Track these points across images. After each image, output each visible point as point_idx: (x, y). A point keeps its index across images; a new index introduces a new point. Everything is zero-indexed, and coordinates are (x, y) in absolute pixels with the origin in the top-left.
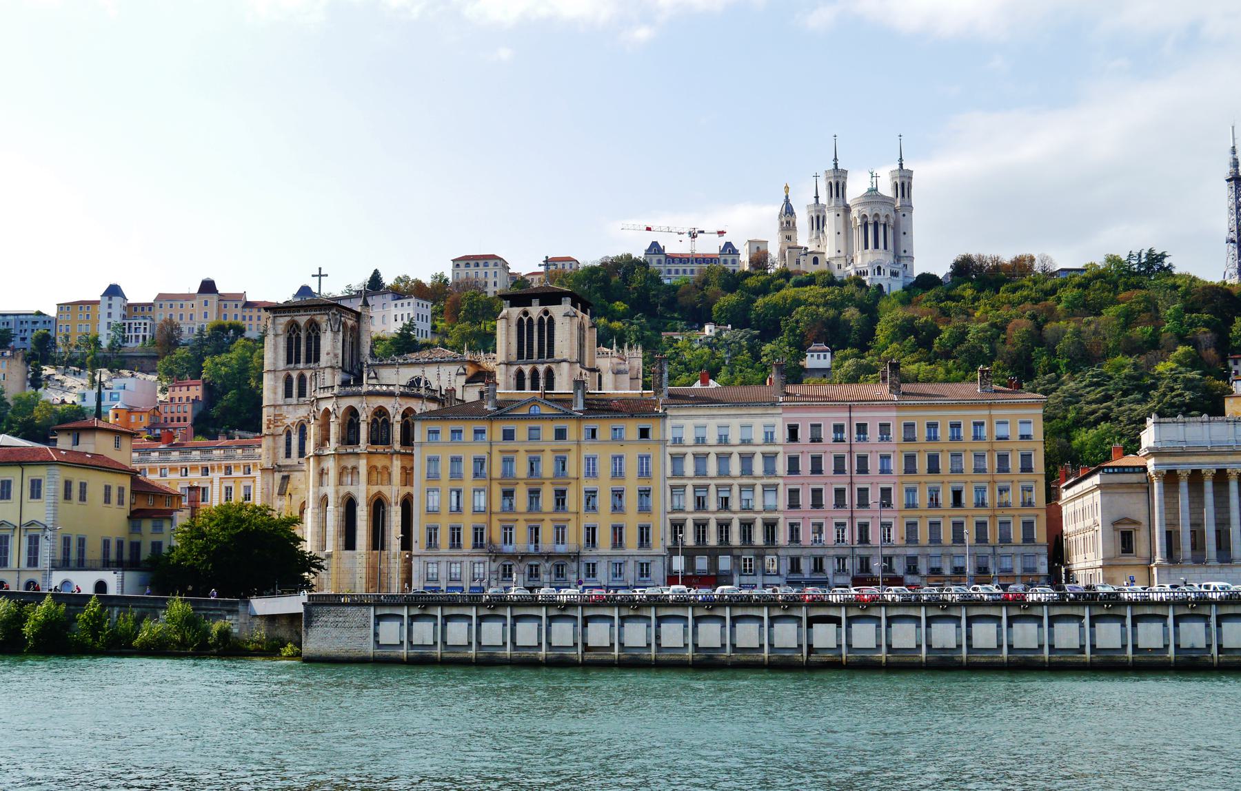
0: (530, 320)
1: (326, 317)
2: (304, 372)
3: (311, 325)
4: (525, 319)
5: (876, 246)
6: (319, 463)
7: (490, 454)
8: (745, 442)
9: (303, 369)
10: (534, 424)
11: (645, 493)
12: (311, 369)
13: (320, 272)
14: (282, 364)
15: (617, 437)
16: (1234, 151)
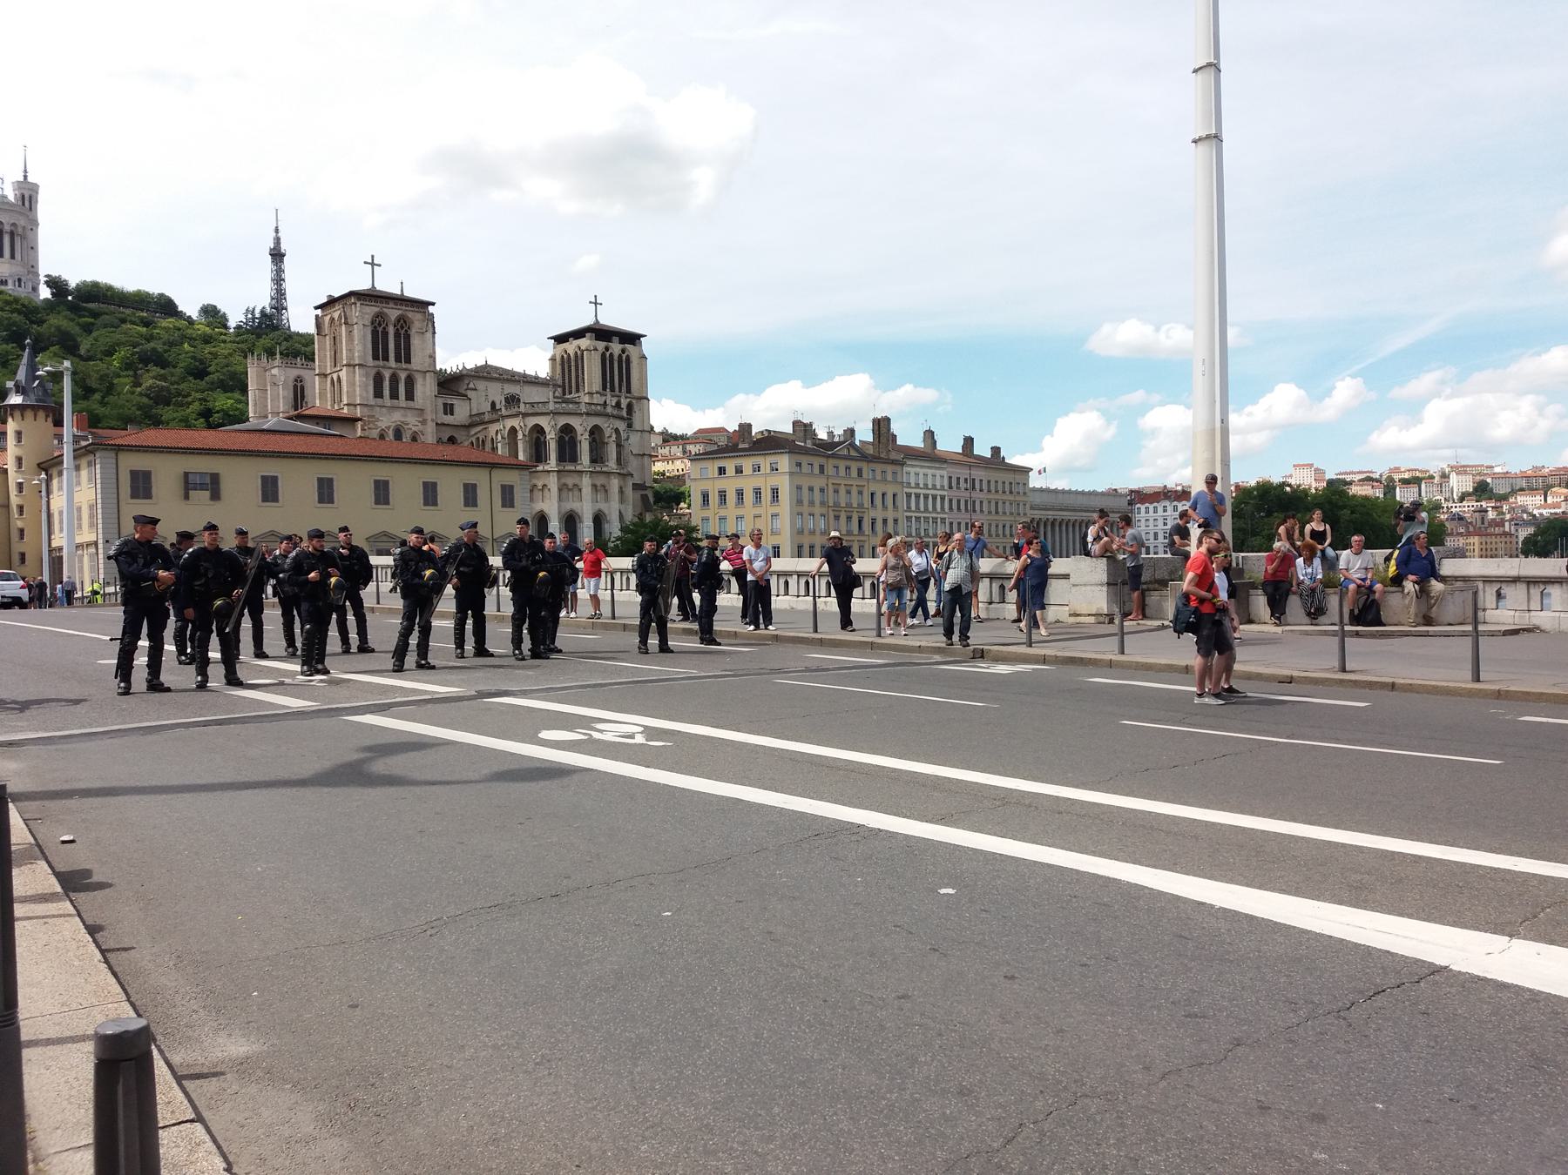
0: (611, 355)
1: (419, 316)
2: (398, 371)
3: (399, 321)
4: (608, 354)
5: (13, 257)
6: (559, 479)
7: (827, 485)
8: (934, 487)
9: (397, 369)
10: (848, 463)
11: (896, 521)
12: (406, 369)
13: (373, 260)
14: (370, 361)
15: (884, 480)
16: (277, 230)
